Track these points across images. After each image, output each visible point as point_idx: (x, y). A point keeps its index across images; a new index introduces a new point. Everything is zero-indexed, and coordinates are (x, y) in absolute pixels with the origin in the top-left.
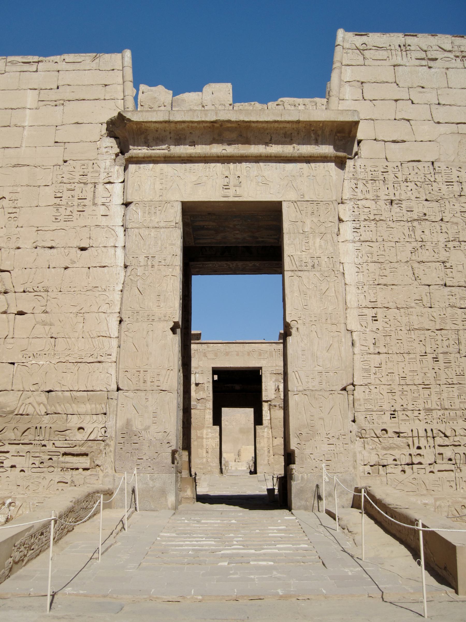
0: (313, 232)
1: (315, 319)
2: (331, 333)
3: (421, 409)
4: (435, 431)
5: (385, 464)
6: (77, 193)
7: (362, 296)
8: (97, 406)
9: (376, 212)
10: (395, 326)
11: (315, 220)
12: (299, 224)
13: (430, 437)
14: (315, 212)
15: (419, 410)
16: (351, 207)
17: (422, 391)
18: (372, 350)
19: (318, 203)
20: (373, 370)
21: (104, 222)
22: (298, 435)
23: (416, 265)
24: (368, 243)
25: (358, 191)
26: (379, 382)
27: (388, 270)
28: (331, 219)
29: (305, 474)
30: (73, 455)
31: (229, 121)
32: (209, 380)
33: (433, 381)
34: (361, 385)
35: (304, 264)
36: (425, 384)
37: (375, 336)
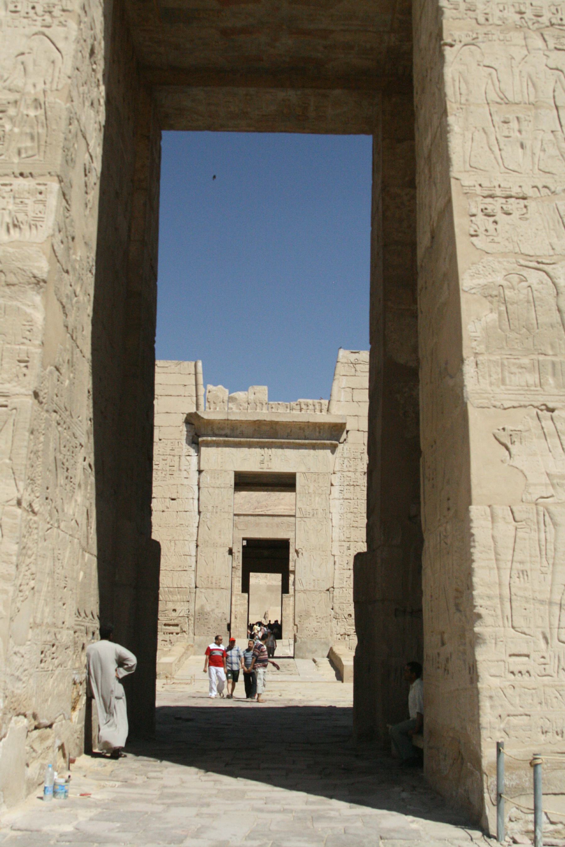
0: (315, 493)
6: (168, 461)
7: (342, 534)
8: (184, 597)
9: (354, 480)
11: (316, 485)
12: (306, 487)
14: (317, 480)
18: (346, 567)
19: (318, 474)
20: (346, 579)
21: (185, 482)
24: (348, 500)
25: (345, 465)
26: (348, 586)
27: (359, 518)
28: (326, 485)
30: (169, 625)
31: (265, 421)
32: (239, 550)
35: (308, 514)
37: (348, 558)
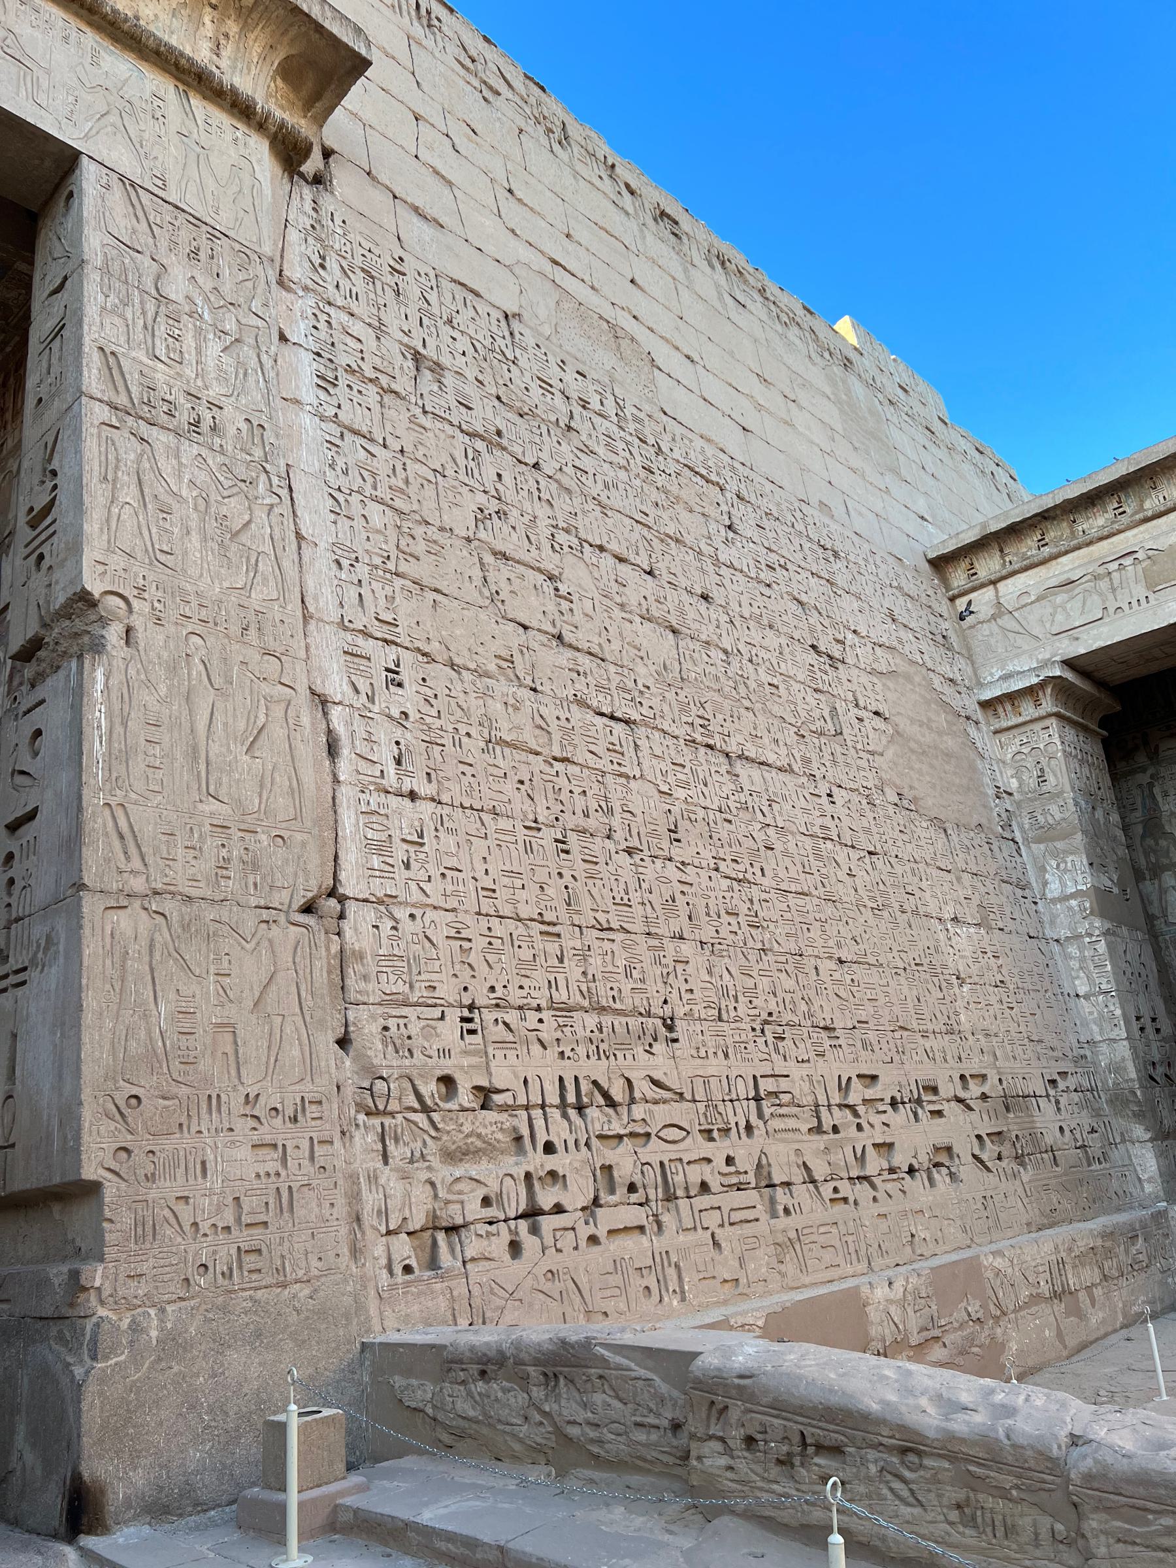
1: (204, 614)
2: (263, 685)
3: (544, 1004)
4: (585, 1087)
5: (459, 1221)
10: (452, 718)
13: (552, 1106)
15: (539, 1009)
16: (309, 312)
17: (539, 943)
20: (400, 852)
22: (122, 1104)
23: (489, 559)
29: (152, 1312)
33: (564, 917)
34: (365, 901)
36: (546, 919)
